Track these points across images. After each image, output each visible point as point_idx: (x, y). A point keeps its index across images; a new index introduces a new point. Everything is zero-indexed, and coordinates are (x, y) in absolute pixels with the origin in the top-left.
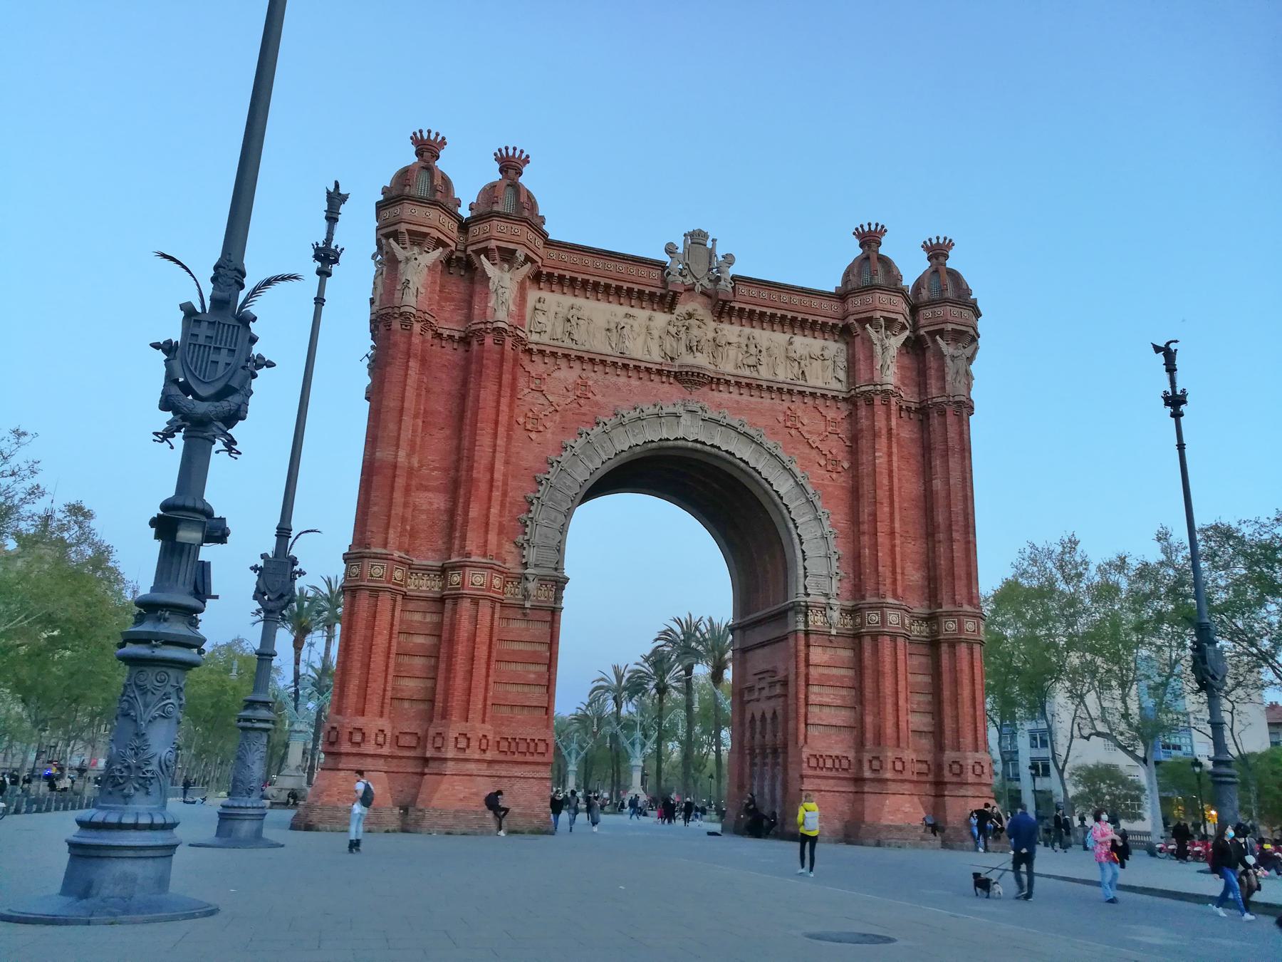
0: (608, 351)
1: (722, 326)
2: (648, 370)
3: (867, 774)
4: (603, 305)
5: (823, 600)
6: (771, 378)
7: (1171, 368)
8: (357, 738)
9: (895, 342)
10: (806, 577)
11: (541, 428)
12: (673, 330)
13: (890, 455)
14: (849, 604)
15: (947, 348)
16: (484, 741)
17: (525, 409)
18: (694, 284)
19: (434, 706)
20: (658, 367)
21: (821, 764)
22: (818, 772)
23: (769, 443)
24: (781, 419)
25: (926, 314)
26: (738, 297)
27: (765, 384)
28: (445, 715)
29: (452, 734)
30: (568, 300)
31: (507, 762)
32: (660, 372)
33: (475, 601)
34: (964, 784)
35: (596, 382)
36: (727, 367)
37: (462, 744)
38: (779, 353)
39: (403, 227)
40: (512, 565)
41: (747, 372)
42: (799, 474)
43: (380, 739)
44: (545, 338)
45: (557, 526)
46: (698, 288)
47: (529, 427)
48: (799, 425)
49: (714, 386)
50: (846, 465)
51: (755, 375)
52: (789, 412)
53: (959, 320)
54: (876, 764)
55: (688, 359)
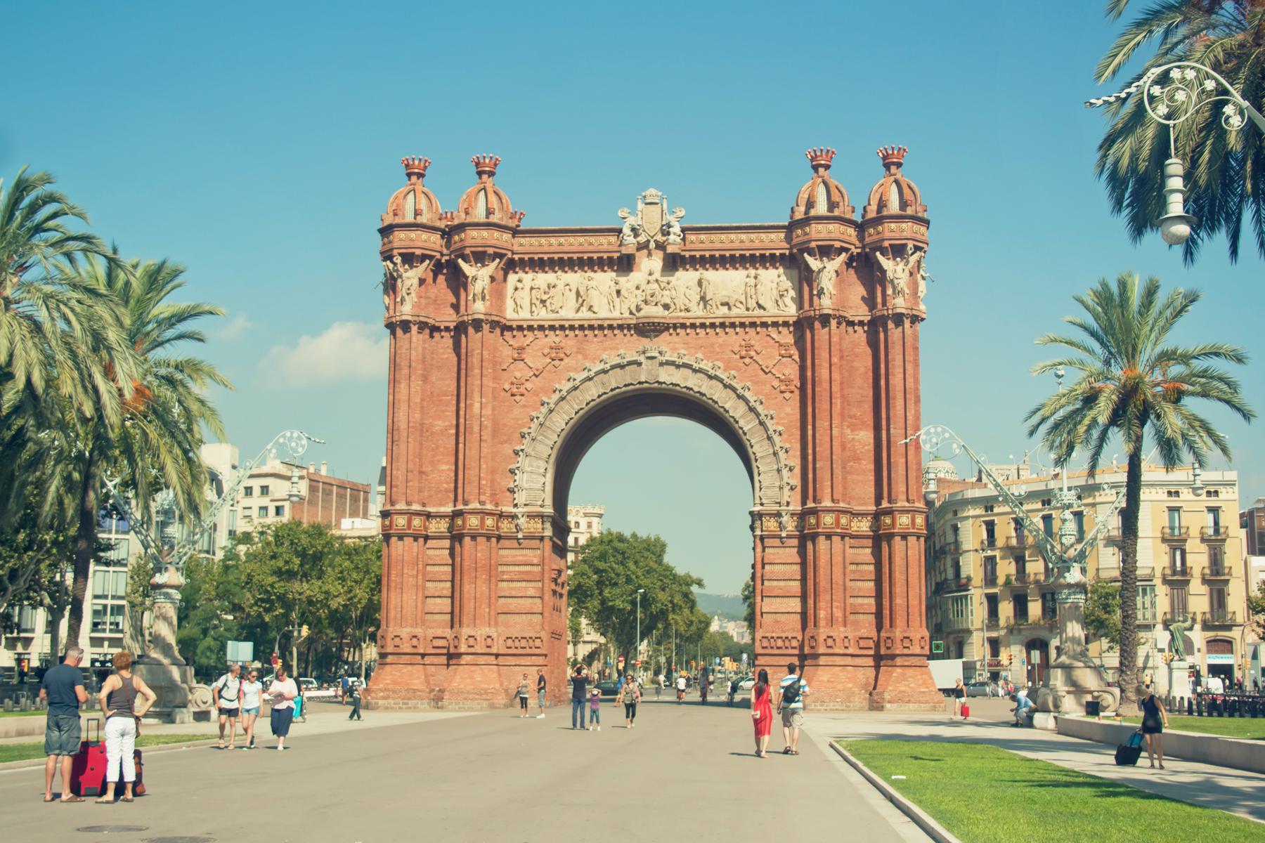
2: (611, 327)
5: (777, 508)
11: (522, 390)
18: (648, 241)
20: (620, 322)
22: (769, 651)
32: (621, 327)
37: (471, 641)
44: (524, 314)
46: (652, 245)
47: (515, 390)
48: (753, 353)
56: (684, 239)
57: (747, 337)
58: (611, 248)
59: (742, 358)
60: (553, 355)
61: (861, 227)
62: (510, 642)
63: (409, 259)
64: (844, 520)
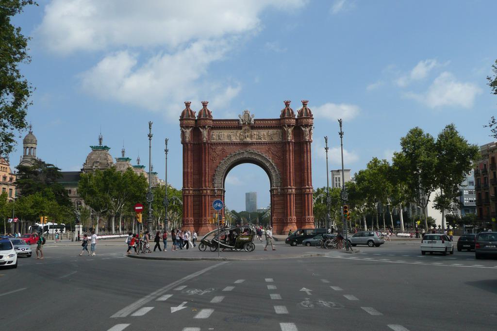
3: (285, 222)
7: (326, 142)
12: (242, 134)
14: (282, 188)
15: (303, 129)
25: (299, 121)
28: (202, 216)
34: (306, 223)
36: (254, 140)
39: (184, 125)
40: (211, 188)
50: (282, 158)
55: (245, 140)
61: (297, 120)
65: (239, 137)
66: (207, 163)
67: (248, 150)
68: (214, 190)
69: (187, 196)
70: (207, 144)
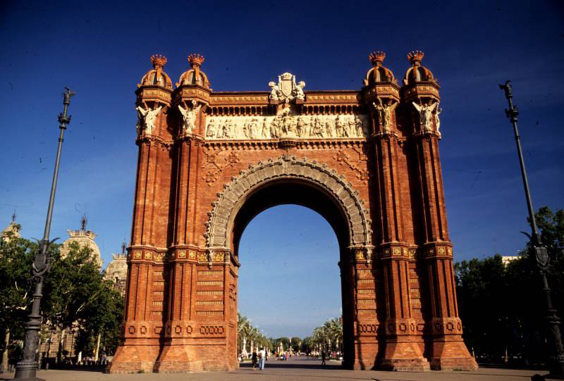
0: (245, 138)
1: (301, 117)
4: (242, 117)
6: (329, 137)
8: (132, 330)
9: (389, 111)
10: (353, 235)
11: (214, 180)
12: (276, 123)
13: (391, 166)
16: (189, 329)
17: (207, 172)
18: (285, 100)
19: (167, 315)
21: (365, 330)
23: (330, 170)
24: (335, 157)
26: (308, 102)
27: (325, 142)
28: (172, 319)
29: (174, 326)
30: (225, 118)
31: (205, 338)
32: (270, 144)
33: (182, 264)
35: (240, 154)
36: (305, 136)
37: (178, 330)
38: (332, 126)
40: (202, 246)
41: (316, 137)
42: (346, 184)
43: (143, 330)
44: (214, 138)
45: (224, 225)
46: (287, 101)
47: (208, 180)
48: (346, 159)
49: (299, 146)
51: (320, 137)
52: (339, 153)
53: (424, 92)
54: (392, 326)
55: (284, 136)
56: (305, 98)
57: (341, 150)
58: (264, 102)
59: (338, 161)
60: (231, 160)
62: (203, 330)
63: (152, 105)
64: (405, 252)
65: (271, 131)
66: (192, 184)
67: (290, 158)
68: (207, 252)
69: (138, 264)
70: (193, 143)
